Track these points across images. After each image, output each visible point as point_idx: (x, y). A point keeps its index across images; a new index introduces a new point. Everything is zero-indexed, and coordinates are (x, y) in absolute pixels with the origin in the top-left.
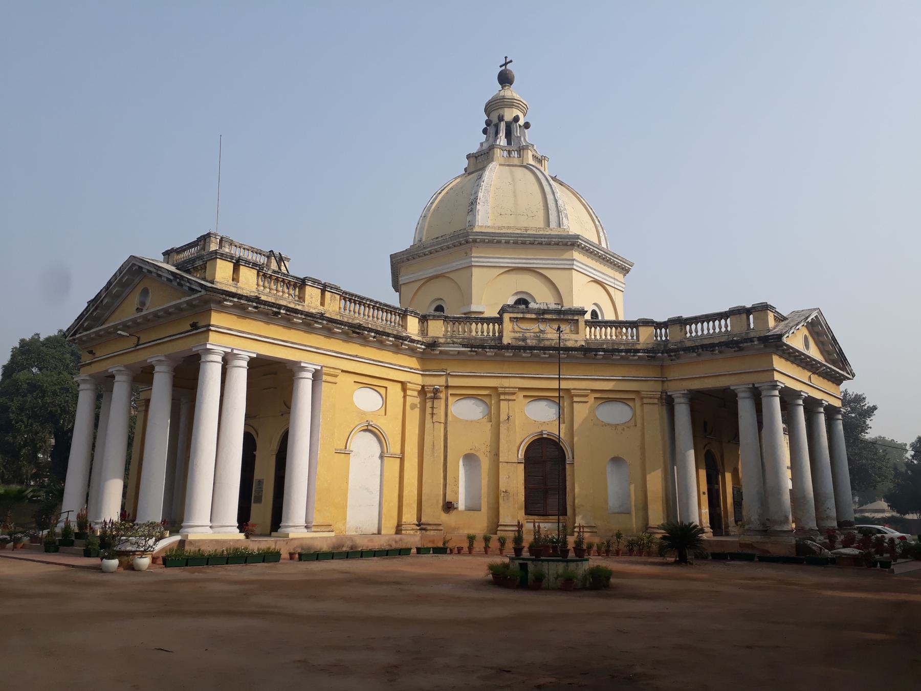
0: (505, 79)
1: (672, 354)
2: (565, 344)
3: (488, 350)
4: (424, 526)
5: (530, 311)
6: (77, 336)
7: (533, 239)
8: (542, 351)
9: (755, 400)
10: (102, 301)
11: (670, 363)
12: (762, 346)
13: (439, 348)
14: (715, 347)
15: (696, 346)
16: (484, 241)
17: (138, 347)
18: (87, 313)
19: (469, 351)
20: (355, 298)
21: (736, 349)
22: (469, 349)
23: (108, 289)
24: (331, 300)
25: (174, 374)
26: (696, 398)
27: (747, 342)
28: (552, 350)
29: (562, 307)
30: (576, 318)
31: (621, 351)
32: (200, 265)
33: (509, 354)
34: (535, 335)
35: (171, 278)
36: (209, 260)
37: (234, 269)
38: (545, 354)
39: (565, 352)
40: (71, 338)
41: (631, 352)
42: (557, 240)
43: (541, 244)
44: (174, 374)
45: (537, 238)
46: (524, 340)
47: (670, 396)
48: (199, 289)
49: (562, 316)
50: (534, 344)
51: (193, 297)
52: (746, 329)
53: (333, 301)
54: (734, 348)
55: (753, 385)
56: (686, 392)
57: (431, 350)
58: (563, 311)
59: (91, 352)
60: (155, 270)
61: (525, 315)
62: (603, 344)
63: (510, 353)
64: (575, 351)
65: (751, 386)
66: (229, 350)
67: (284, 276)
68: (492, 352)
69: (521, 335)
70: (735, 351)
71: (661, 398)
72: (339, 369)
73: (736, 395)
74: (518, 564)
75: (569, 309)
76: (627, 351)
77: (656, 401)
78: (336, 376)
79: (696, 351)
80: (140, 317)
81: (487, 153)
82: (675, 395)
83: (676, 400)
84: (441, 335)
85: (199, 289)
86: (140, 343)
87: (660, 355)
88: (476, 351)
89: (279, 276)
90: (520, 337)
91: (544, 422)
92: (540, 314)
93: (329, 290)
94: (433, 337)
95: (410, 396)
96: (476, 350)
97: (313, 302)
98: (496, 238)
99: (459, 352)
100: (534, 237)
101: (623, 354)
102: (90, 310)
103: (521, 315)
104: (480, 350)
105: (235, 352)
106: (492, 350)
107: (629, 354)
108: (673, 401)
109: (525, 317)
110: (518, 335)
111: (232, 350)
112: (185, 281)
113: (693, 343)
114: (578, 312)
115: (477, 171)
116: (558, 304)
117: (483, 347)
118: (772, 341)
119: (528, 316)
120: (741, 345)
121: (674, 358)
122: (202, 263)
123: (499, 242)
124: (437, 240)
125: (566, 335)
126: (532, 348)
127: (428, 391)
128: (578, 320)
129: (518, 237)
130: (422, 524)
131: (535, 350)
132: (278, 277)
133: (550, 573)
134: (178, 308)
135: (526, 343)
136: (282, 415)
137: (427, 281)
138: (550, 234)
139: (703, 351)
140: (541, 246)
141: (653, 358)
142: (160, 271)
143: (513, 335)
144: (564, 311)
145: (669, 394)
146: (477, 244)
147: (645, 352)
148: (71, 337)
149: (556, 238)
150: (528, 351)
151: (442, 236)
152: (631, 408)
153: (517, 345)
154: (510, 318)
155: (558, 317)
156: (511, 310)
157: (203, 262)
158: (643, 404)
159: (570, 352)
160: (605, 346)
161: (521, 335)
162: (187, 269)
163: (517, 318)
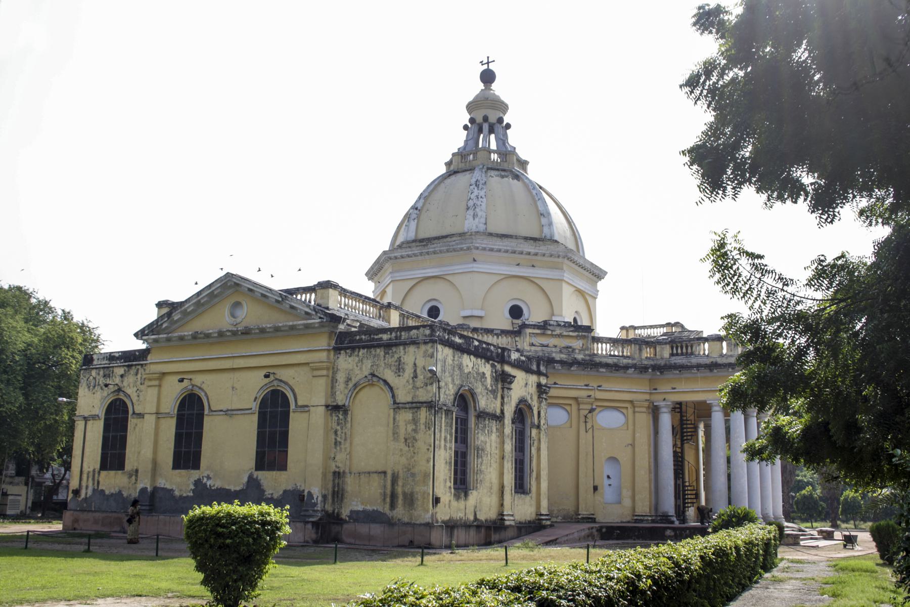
0: (488, 77)
26: (678, 408)
47: (656, 406)
71: (648, 407)
77: (644, 410)
145: (655, 404)
152: (624, 414)
158: (634, 412)
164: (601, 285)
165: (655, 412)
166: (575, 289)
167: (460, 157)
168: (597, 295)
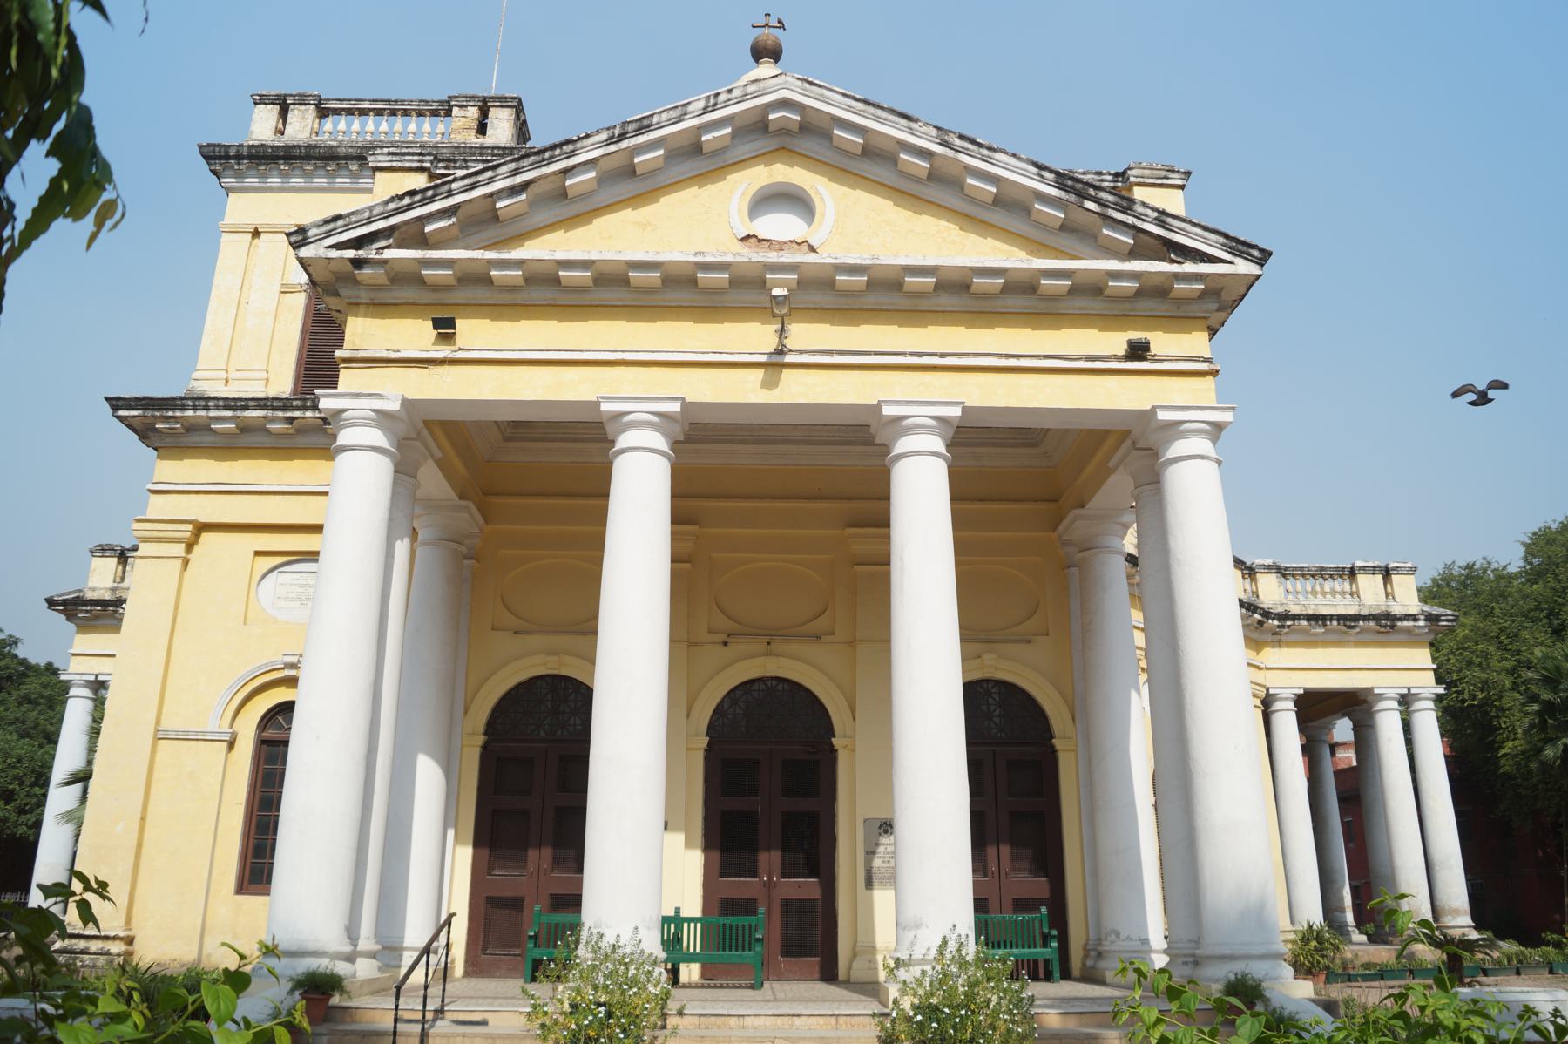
1: (1289, 623)
12: (1427, 630)
14: (1358, 620)
15: (1332, 616)
21: (1388, 629)
23: (622, 137)
27: (1407, 620)
36: (1139, 184)
54: (1385, 626)
79: (1328, 623)
87: (1270, 621)
102: (490, 181)
118: (1445, 623)
120: (1399, 624)
139: (1339, 624)
145: (1271, 691)
148: (339, 246)
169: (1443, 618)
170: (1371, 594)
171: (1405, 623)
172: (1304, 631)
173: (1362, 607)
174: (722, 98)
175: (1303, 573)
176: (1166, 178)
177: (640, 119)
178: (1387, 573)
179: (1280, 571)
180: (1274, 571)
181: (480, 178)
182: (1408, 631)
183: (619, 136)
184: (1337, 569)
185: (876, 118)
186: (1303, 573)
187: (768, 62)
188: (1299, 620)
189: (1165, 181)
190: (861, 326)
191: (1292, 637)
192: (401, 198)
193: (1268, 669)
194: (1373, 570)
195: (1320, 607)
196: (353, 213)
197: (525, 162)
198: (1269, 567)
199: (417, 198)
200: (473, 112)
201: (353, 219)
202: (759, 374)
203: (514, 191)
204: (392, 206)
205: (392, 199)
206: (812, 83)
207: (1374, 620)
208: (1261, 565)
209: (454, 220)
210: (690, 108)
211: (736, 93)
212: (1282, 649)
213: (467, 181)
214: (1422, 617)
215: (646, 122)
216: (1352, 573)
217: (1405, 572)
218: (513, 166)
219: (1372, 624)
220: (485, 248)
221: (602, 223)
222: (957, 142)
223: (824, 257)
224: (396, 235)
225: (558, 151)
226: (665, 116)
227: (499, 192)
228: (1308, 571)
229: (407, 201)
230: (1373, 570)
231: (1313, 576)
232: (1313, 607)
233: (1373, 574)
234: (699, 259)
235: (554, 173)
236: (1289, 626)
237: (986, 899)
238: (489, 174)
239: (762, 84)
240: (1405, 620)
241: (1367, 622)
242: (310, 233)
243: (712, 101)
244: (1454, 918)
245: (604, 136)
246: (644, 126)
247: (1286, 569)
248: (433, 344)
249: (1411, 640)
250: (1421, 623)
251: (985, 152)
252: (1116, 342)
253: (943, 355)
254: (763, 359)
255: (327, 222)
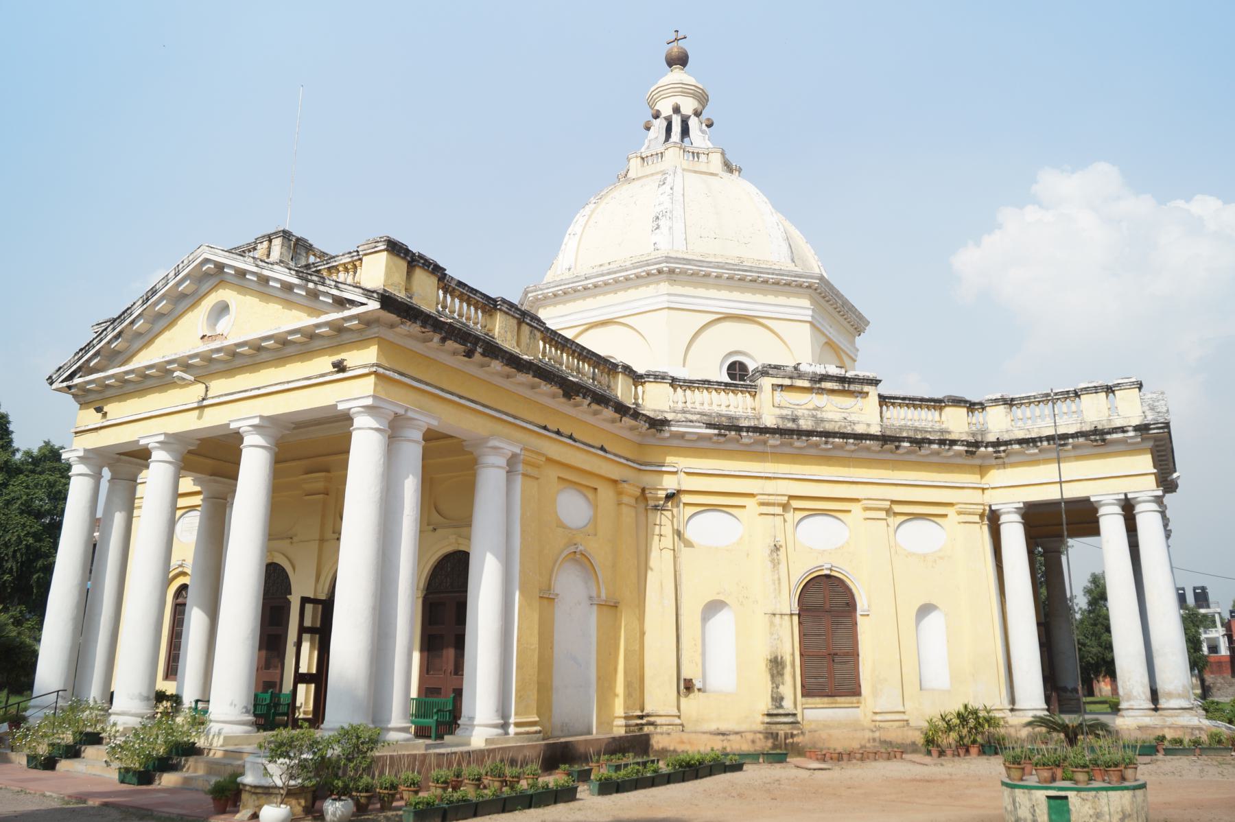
1: (1002, 448)
2: (853, 429)
3: (745, 434)
4: (652, 719)
5: (801, 376)
6: (77, 381)
7: (757, 275)
8: (824, 439)
9: (1126, 520)
10: (133, 322)
11: (994, 462)
12: (1139, 440)
13: (673, 429)
14: (1068, 438)
16: (686, 273)
17: (205, 403)
18: (101, 340)
19: (715, 435)
20: (558, 338)
21: (1100, 443)
22: (716, 431)
23: (148, 299)
24: (530, 338)
25: (277, 450)
27: (1116, 433)
28: (839, 438)
29: (846, 372)
30: (866, 388)
31: (931, 442)
32: (344, 264)
33: (774, 441)
34: (810, 414)
35: (296, 281)
36: (365, 255)
37: (408, 272)
38: (826, 443)
39: (856, 442)
40: (65, 384)
41: (945, 444)
42: (789, 278)
43: (765, 282)
44: (277, 450)
45: (761, 273)
46: (794, 420)
48: (364, 300)
49: (846, 385)
50: (810, 428)
51: (347, 313)
52: (1107, 415)
53: (532, 340)
54: (1096, 441)
55: (1126, 495)
56: (1021, 505)
57: (657, 430)
58: (847, 378)
59: (99, 410)
60: (255, 269)
61: (794, 380)
62: (901, 429)
63: (777, 440)
64: (870, 440)
65: (1122, 497)
66: (401, 411)
67: (470, 292)
68: (751, 437)
69: (790, 413)
70: (1095, 446)
72: (543, 455)
73: (1096, 510)
74: (1044, 799)
75: (856, 375)
76: (942, 442)
77: (977, 519)
78: (538, 467)
79: (1039, 444)
80: (218, 350)
81: (662, 153)
82: (1004, 508)
83: (1003, 519)
84: (667, 409)
85: (364, 300)
86: (210, 394)
87: (983, 449)
88: (725, 435)
89: (464, 291)
90: (789, 415)
91: (824, 551)
92: (815, 382)
93: (528, 321)
94: (655, 411)
95: (626, 505)
96: (727, 432)
97: (508, 339)
98: (704, 269)
99: (701, 437)
100: (759, 272)
101: (935, 447)
102: (106, 336)
103: (787, 382)
104: (733, 433)
105: (410, 414)
106: (750, 434)
107: (943, 447)
108: (998, 518)
109: (794, 384)
110: (785, 412)
111: (407, 410)
112: (329, 286)
113: (1028, 433)
114: (869, 381)
115: (647, 176)
116: (841, 367)
117: (739, 429)
119: (799, 383)
120: (1108, 437)
121: (1003, 455)
122: (350, 260)
123: (707, 275)
124: (602, 268)
125: (853, 415)
126: (809, 433)
127: (650, 497)
128: (867, 393)
129: (734, 270)
130: (648, 715)
131: (813, 436)
132: (463, 293)
133: (1112, 810)
134: (310, 335)
135: (798, 425)
136: (435, 529)
137: (587, 330)
138: (781, 269)
139: (1049, 444)
140: (767, 286)
141: (973, 453)
142: (271, 270)
143: (778, 412)
144: (850, 378)
145: (994, 508)
146: (674, 276)
147: (963, 445)
148: (62, 382)
149: (788, 276)
150: (804, 438)
151: (609, 263)
153: (785, 427)
154: (773, 385)
155: (841, 388)
156: (771, 371)
157: (353, 257)
159: (864, 441)
160: (905, 434)
161: (790, 413)
162: (314, 269)
163: (782, 386)
164: (859, 341)
165: (993, 520)
166: (825, 340)
167: (639, 159)
168: (856, 356)
169: (1152, 426)
170: (1093, 411)
171: (1115, 436)
172: (1017, 453)
173: (1083, 424)
174: (180, 267)
175: (1029, 401)
176: (376, 247)
177: (152, 289)
178: (1109, 390)
179: (1009, 403)
180: (1001, 403)
181: (102, 336)
182: (1123, 442)
183: (146, 299)
184: (1062, 393)
185: (234, 259)
186: (1029, 401)
187: (676, 68)
188: (1011, 444)
189: (376, 249)
190: (261, 371)
191: (1013, 459)
192: (78, 353)
193: (992, 488)
194: (1096, 390)
195: (1043, 429)
196: (64, 365)
197: (115, 324)
198: (996, 400)
199: (83, 351)
200: (266, 244)
201: (65, 367)
202: (196, 412)
203: (116, 337)
204: (76, 357)
205: (75, 355)
206: (212, 248)
207: (1082, 436)
208: (988, 400)
209: (99, 358)
210: (169, 276)
211: (185, 262)
212: (1006, 470)
213: (98, 339)
214: (1131, 428)
215: (154, 289)
216: (1109, 390)
217: (1129, 387)
218: (112, 326)
219: (1081, 440)
220: (120, 366)
221: (160, 341)
222: (260, 263)
223: (231, 341)
224: (84, 370)
225: (126, 315)
226: (160, 284)
227: (111, 340)
228: (1035, 398)
229: (80, 354)
230: (1096, 390)
231: (1039, 402)
232: (1036, 430)
233: (1096, 393)
234: (167, 359)
235: (127, 325)
236: (1004, 451)
237: (441, 689)
238: (105, 333)
239: (195, 254)
240: (1113, 433)
241: (1076, 440)
242: (53, 378)
243: (177, 270)
244: (1168, 700)
245: (140, 302)
246: (154, 291)
247: (1012, 400)
248: (102, 418)
249: (1129, 449)
250: (1131, 434)
251: (270, 266)
252: (323, 364)
253: (259, 388)
254: (195, 405)
255: (58, 371)
